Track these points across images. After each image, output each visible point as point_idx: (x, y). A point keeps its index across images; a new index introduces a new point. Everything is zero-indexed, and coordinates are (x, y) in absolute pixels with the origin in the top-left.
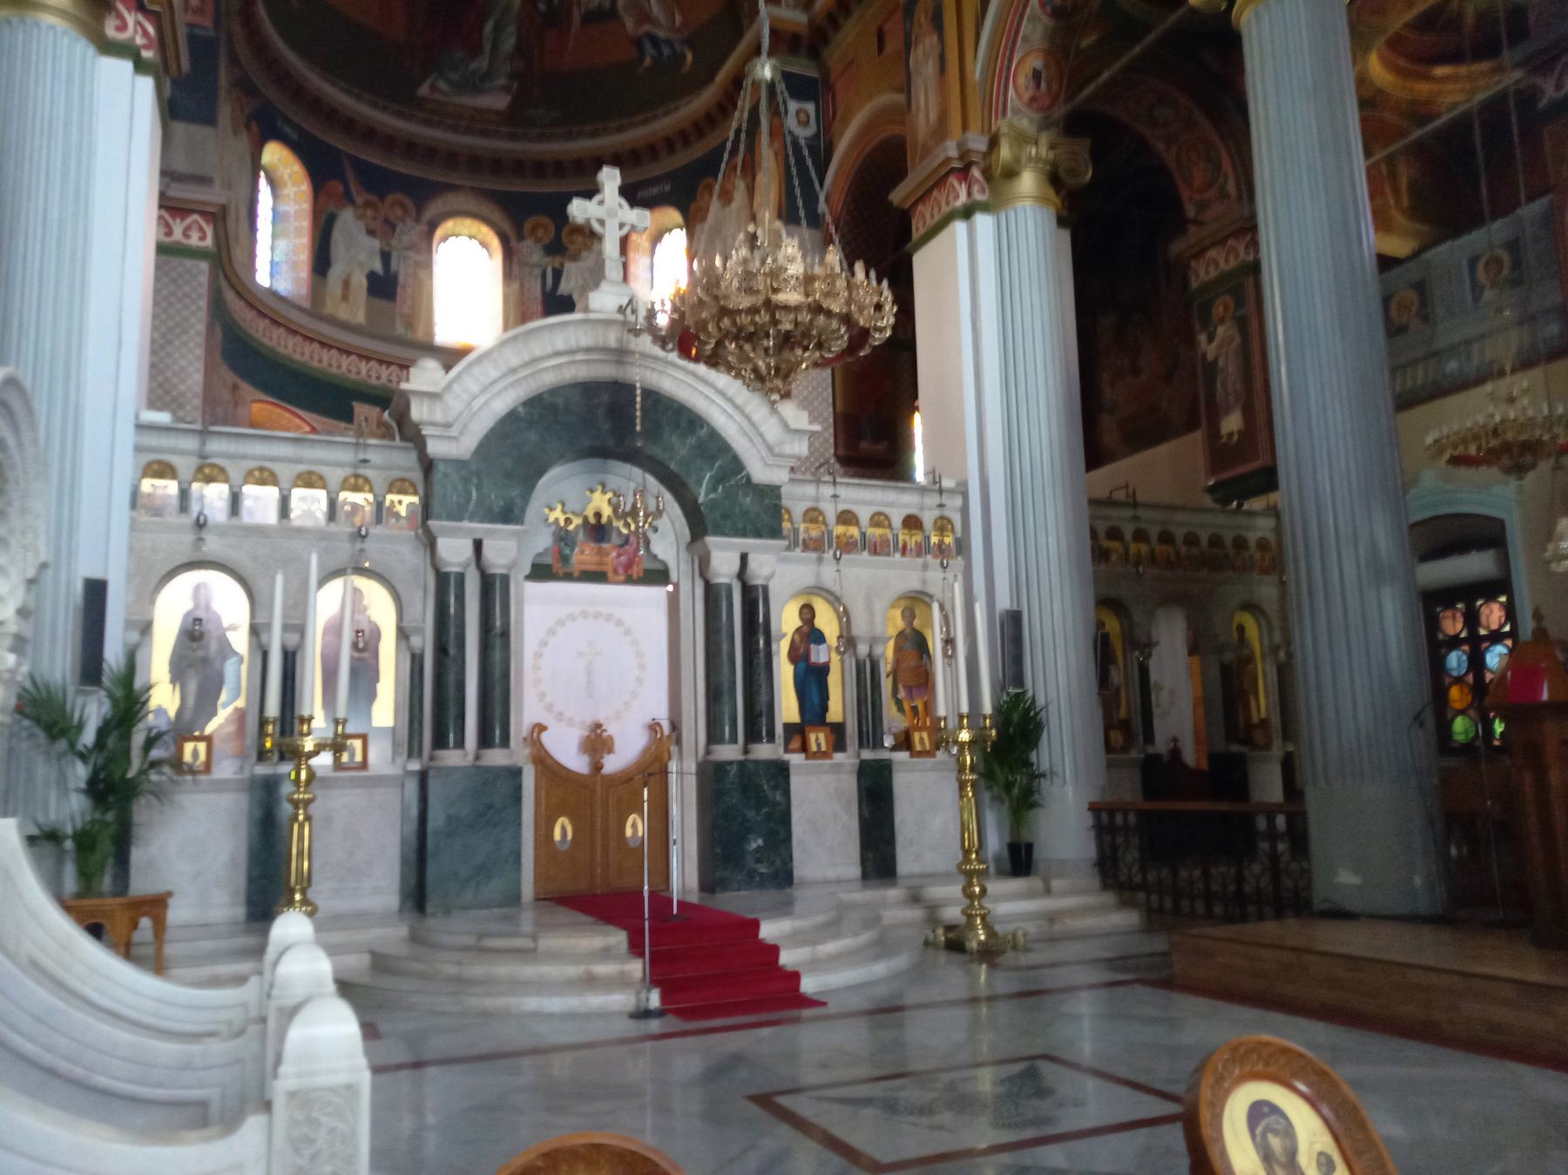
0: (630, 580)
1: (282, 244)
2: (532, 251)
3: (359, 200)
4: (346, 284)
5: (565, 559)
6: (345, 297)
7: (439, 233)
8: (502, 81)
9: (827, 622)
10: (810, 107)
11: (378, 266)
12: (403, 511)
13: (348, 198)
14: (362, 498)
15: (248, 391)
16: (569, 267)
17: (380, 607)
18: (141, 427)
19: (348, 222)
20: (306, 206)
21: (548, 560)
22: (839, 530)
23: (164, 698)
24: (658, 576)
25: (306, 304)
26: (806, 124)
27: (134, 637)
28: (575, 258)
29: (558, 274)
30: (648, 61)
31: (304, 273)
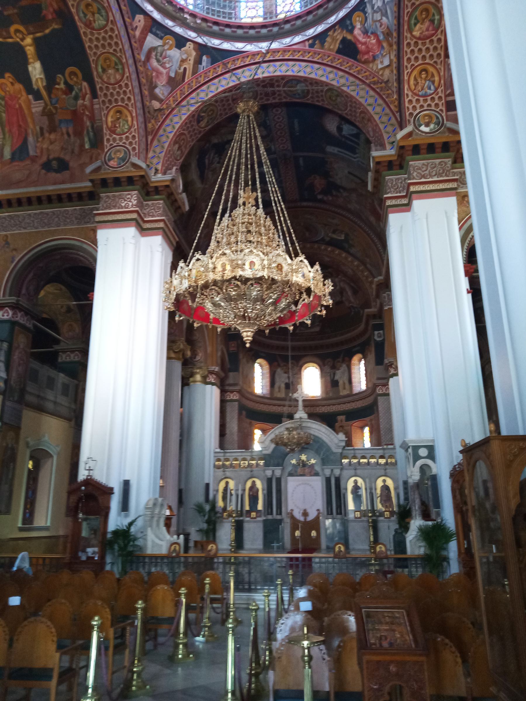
0: (311, 476)
1: (264, 381)
2: (327, 369)
3: (282, 365)
4: (279, 388)
5: (296, 471)
6: (279, 391)
7: (303, 368)
8: (317, 324)
9: (360, 481)
10: (381, 332)
11: (287, 381)
12: (261, 464)
13: (279, 366)
14: (254, 462)
15: (254, 422)
16: (337, 372)
17: (259, 484)
18: (216, 453)
19: (279, 371)
20: (268, 371)
21: (292, 472)
22: (362, 461)
23: (220, 503)
24: (317, 474)
25: (268, 396)
26: (380, 337)
27: (215, 492)
28: (339, 369)
29: (334, 374)
30: (353, 313)
31: (268, 388)
